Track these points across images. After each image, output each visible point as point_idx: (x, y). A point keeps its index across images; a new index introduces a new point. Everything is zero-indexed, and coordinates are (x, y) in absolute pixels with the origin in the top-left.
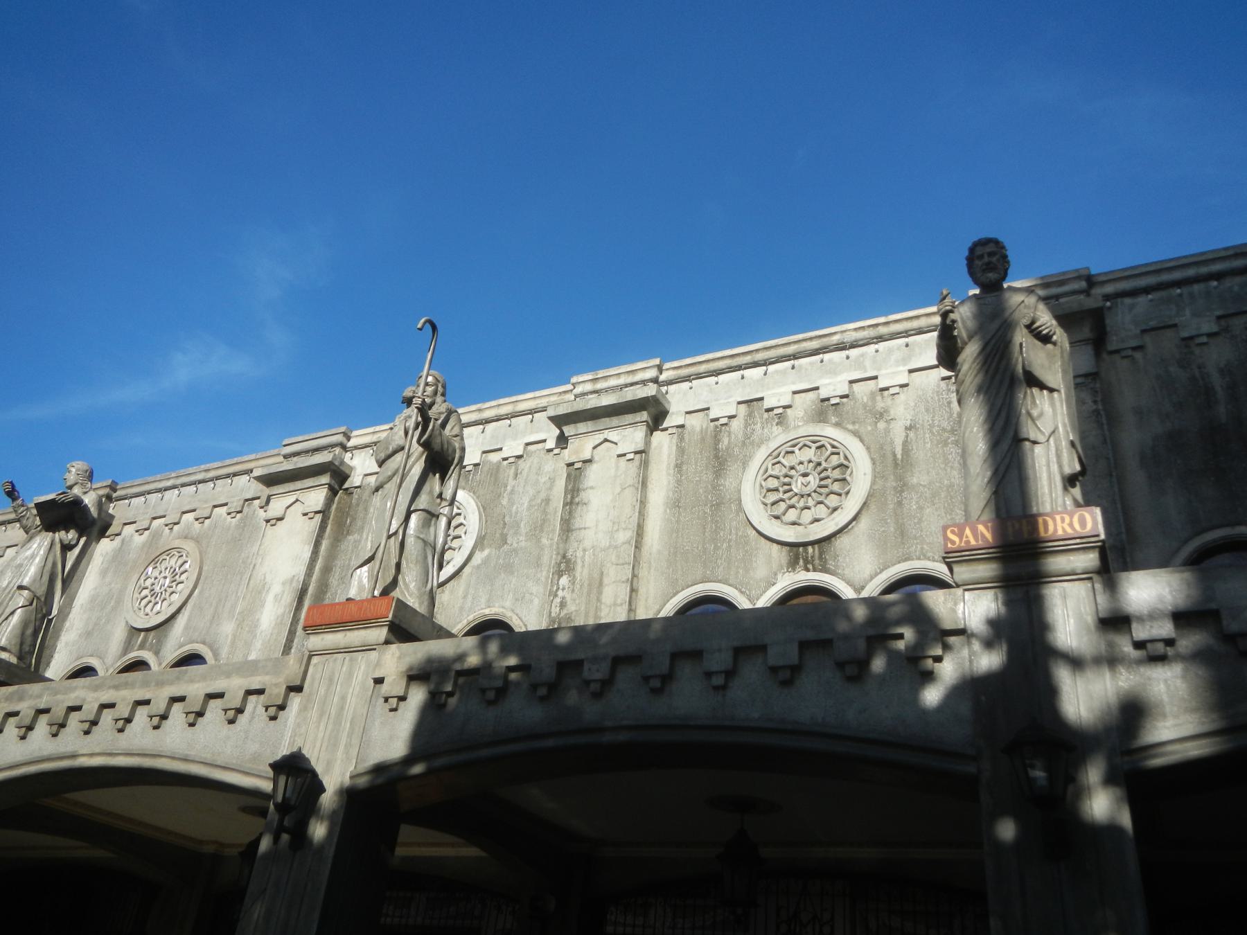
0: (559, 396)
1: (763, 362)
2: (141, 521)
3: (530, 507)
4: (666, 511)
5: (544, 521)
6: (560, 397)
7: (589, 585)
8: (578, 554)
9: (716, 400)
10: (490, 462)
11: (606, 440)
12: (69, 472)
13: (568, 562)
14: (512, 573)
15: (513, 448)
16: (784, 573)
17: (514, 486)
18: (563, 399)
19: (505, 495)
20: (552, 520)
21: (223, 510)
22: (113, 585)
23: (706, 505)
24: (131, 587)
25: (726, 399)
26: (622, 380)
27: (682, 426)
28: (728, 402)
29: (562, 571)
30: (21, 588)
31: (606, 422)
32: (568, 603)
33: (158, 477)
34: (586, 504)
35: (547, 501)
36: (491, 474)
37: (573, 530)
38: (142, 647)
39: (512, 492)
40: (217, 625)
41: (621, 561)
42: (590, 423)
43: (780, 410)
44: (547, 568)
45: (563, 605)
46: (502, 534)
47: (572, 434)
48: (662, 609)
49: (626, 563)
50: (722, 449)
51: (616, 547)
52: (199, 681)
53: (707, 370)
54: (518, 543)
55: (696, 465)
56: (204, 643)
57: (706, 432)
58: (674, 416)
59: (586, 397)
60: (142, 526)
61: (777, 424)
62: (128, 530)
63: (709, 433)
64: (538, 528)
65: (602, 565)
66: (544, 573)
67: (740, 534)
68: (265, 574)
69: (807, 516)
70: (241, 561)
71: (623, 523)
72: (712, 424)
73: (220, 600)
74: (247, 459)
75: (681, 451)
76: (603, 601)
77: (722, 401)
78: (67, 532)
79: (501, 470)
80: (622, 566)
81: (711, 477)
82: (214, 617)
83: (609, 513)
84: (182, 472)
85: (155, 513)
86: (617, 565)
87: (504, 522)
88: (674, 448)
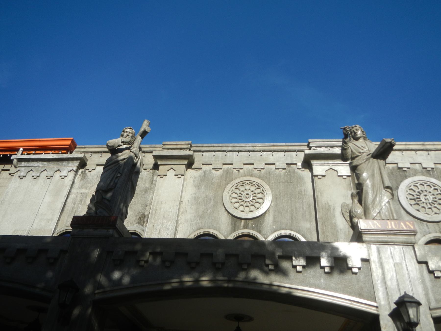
2: (215, 164)
21: (273, 167)
22: (208, 194)
30: (388, 187)
33: (220, 145)
38: (246, 227)
40: (297, 222)
56: (291, 230)
60: (218, 167)
62: (205, 168)
68: (327, 201)
69: (241, 208)
70: (297, 193)
73: (292, 210)
82: (292, 218)
84: (236, 145)
85: (224, 161)
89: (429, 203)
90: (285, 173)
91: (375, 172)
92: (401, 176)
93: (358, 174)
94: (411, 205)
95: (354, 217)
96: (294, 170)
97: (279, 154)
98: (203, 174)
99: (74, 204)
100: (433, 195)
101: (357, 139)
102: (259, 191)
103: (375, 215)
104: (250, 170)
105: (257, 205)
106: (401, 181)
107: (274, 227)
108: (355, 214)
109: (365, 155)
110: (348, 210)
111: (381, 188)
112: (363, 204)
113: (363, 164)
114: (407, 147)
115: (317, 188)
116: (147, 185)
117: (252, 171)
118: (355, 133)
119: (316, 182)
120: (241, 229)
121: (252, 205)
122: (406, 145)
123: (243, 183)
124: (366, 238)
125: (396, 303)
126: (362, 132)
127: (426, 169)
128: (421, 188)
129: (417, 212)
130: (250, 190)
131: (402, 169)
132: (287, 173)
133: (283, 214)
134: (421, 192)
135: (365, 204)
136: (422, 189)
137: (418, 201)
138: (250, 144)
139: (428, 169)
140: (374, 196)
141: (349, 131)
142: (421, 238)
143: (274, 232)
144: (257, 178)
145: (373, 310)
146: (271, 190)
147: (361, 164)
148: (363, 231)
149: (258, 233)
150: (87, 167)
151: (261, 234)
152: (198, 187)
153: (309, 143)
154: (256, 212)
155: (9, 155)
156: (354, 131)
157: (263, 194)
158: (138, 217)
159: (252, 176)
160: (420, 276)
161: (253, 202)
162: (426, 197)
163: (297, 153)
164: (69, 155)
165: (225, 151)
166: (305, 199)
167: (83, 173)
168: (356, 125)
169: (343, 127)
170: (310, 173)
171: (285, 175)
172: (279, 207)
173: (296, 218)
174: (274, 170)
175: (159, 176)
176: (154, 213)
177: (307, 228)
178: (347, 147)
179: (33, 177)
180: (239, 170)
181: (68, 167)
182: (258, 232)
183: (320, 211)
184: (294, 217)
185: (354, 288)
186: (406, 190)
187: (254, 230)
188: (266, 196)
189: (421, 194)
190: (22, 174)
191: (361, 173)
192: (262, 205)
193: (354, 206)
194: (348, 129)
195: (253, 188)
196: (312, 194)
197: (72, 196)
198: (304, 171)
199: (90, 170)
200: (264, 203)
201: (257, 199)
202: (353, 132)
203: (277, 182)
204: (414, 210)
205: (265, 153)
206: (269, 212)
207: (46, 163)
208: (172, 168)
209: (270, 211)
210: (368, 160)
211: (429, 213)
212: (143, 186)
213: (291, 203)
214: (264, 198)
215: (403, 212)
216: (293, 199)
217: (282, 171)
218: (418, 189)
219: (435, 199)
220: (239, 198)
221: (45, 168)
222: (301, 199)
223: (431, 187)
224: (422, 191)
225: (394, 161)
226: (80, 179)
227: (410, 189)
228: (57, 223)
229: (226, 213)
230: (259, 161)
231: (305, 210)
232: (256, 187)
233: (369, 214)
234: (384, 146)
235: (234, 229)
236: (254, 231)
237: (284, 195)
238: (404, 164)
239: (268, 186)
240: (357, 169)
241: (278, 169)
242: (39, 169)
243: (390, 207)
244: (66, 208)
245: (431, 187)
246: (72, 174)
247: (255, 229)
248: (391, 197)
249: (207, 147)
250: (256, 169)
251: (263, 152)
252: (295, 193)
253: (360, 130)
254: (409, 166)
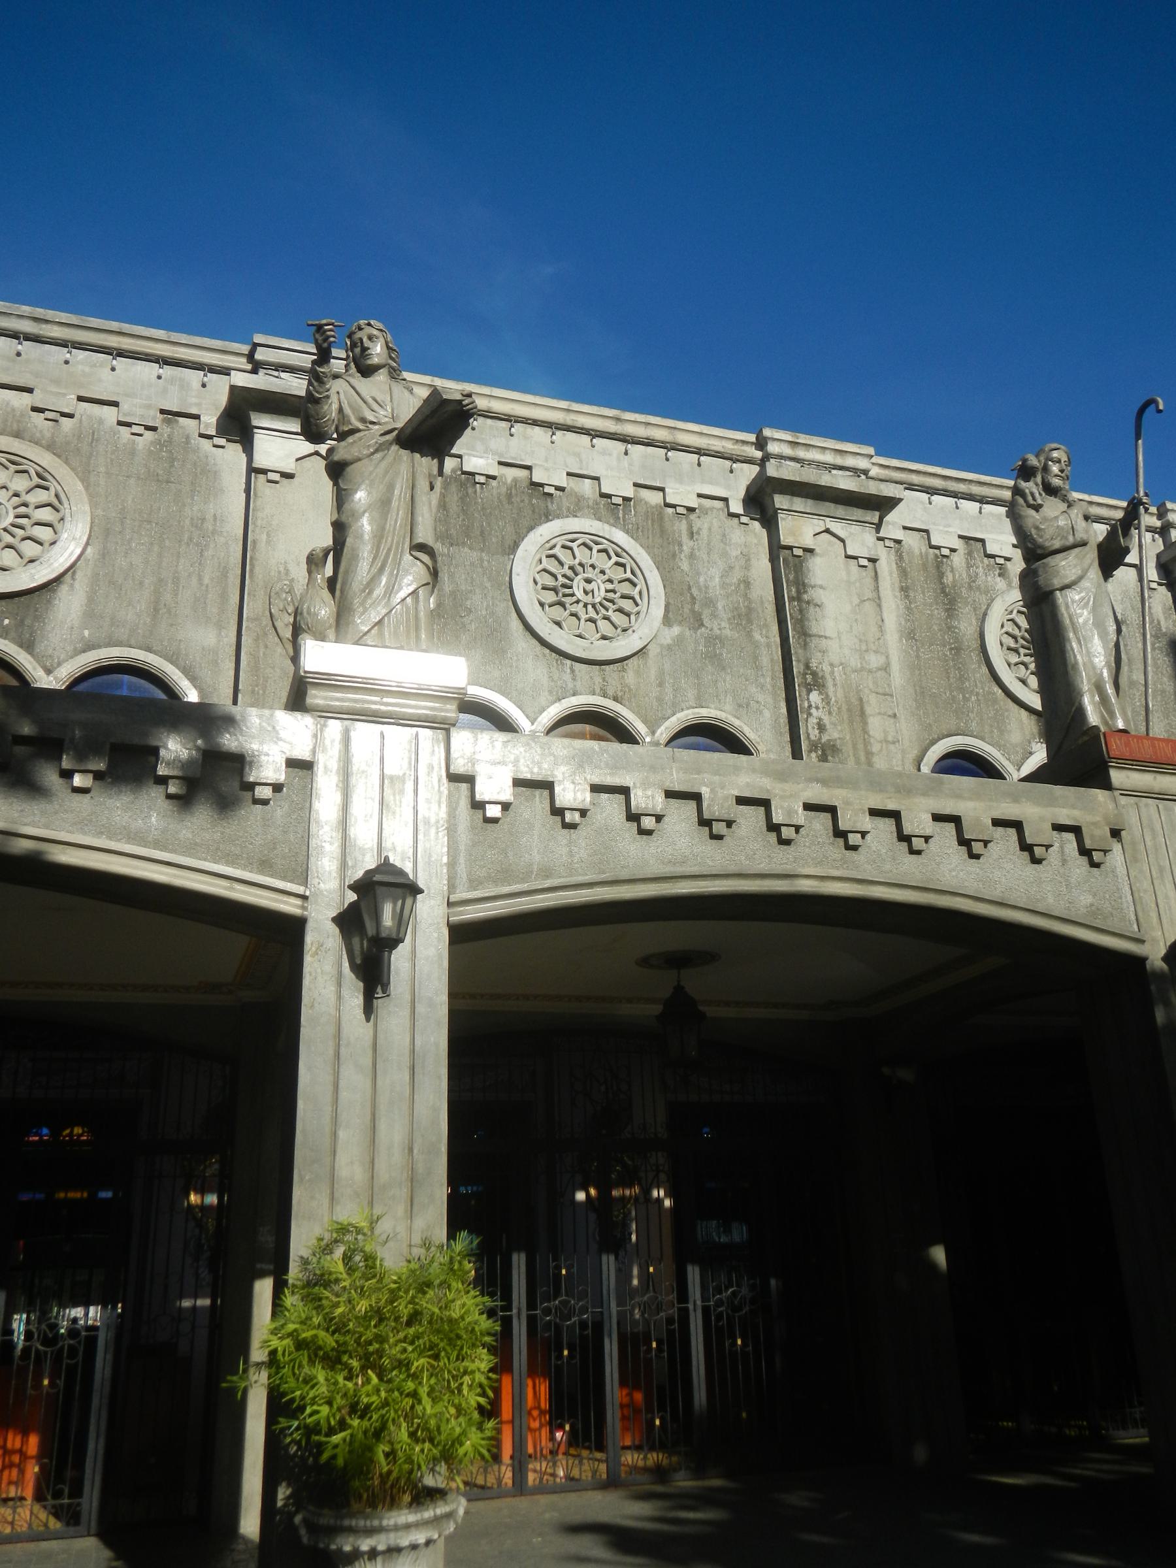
0: (733, 444)
1: (978, 498)
3: (724, 585)
4: (901, 640)
5: (750, 610)
6: (736, 447)
7: (849, 710)
8: (824, 668)
9: (934, 524)
10: (646, 503)
11: (827, 531)
12: (370, 338)
13: (814, 674)
14: (724, 669)
15: (682, 494)
16: (1037, 743)
17: (693, 549)
18: (744, 451)
19: (682, 556)
20: (760, 612)
23: (944, 646)
25: (945, 527)
26: (829, 458)
27: (898, 542)
28: (947, 531)
29: (809, 684)
30: (422, 547)
31: (829, 508)
32: (828, 727)
34: (818, 606)
35: (747, 583)
36: (653, 521)
37: (810, 636)
39: (692, 556)
40: (172, 625)
41: (881, 691)
42: (810, 502)
43: (1001, 561)
44: (770, 673)
45: (821, 727)
46: (692, 611)
47: (785, 508)
48: (924, 756)
49: (888, 695)
50: (948, 585)
51: (870, 671)
52: (971, 799)
53: (921, 483)
54: (720, 629)
55: (923, 593)
56: (149, 650)
57: (927, 558)
58: (890, 526)
59: (783, 461)
61: (1000, 575)
63: (930, 560)
64: (744, 617)
65: (858, 691)
66: (768, 680)
67: (986, 689)
70: (187, 522)
71: (872, 645)
72: (931, 551)
74: (144, 334)
75: (903, 573)
76: (871, 733)
77: (941, 528)
78: (433, 459)
79: (667, 519)
80: (884, 697)
81: (943, 615)
82: (156, 610)
83: (851, 627)
86: (877, 693)
87: (692, 595)
88: (894, 566)
89: (594, 606)
90: (152, 443)
91: (396, 492)
92: (533, 511)
93: (343, 492)
94: (542, 605)
95: (304, 631)
96: (188, 437)
97: (139, 368)
100: (610, 581)
101: (367, 371)
102: (41, 496)
103: (365, 629)
104: (13, 410)
105: (29, 549)
106: (531, 528)
107: (86, 633)
108: (309, 620)
109: (377, 430)
110: (294, 604)
111: (403, 548)
112: (338, 593)
113: (363, 461)
114: (570, 419)
115: (259, 514)
117: (22, 415)
118: (364, 349)
119: (259, 494)
122: (568, 410)
124: (315, 697)
125: (354, 887)
126: (388, 348)
127: (609, 500)
128: (581, 555)
129: (556, 628)
130: (8, 490)
131: (541, 489)
132: (162, 446)
133: (126, 590)
134: (580, 569)
135: (342, 591)
136: (584, 561)
137: (565, 595)
138: (26, 309)
139: (615, 500)
140: (374, 570)
141: (332, 339)
142: (548, 707)
143: (84, 651)
144: (41, 446)
145: (289, 906)
146: (90, 502)
147: (359, 460)
148: (311, 675)
149: (20, 650)
151: (35, 653)
153: (255, 346)
154: (23, 576)
156: (361, 340)
157: (58, 511)
159: (23, 439)
160: (445, 816)
161: (13, 536)
162: (589, 587)
163: (205, 375)
166: (212, 546)
168: (372, 322)
169: (317, 322)
170: (243, 458)
171: (150, 452)
172: (114, 565)
173: (169, 612)
174: (111, 428)
177: (203, 649)
178: (323, 392)
182: (21, 646)
183: (254, 596)
184: (165, 605)
185: (251, 844)
186: (537, 557)
187: (5, 639)
188: (68, 518)
189: (576, 574)
191: (351, 489)
192: (48, 551)
193: (309, 595)
194: (332, 333)
195: (20, 484)
196: (241, 531)
198: (223, 447)
200: (58, 543)
201: (32, 526)
202: (359, 344)
203: (117, 475)
204: (546, 620)
205: (81, 355)
206: (73, 579)
209: (79, 575)
210: (383, 450)
211: (587, 636)
213: (160, 555)
214: (58, 526)
215: (515, 623)
216: (167, 543)
217: (141, 435)
218: (575, 558)
219: (611, 595)
222: (197, 545)
223: (610, 558)
224: (581, 564)
225: (521, 460)
227: (548, 556)
230: (57, 382)
231: (207, 586)
232: (31, 480)
233: (348, 624)
234: (434, 412)
236: (6, 642)
237: (137, 523)
238: (551, 474)
239: (79, 483)
240: (345, 473)
241: (129, 425)
243: (416, 609)
245: (610, 558)
247: (13, 634)
248: (426, 578)
250: (40, 410)
251: (73, 350)
252: (179, 522)
253: (382, 340)
254: (562, 481)
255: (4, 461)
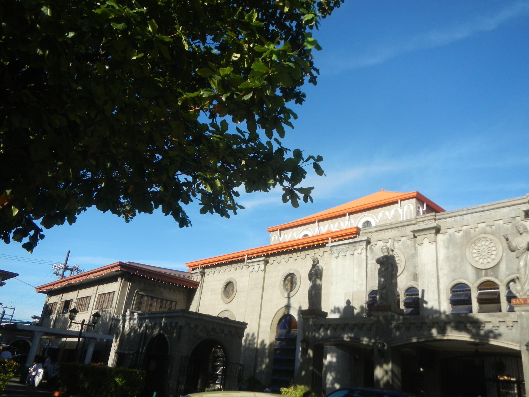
21: (501, 222)
24: (468, 254)
38: (486, 275)
62: (450, 231)
74: (503, 202)
98: (449, 237)
99: (372, 271)
102: (492, 245)
116: (413, 251)
120: (483, 277)
121: (489, 257)
123: (479, 240)
140: (525, 280)
150: (372, 243)
152: (447, 248)
155: (324, 243)
158: (413, 276)
164: (358, 239)
165: (461, 215)
167: (371, 248)
175: (418, 244)
176: (421, 272)
179: (343, 256)
180: (474, 229)
181: (360, 246)
190: (336, 255)
197: (369, 266)
199: (374, 246)
207: (346, 246)
208: (426, 237)
212: (410, 252)
220: (479, 252)
221: (348, 249)
226: (370, 253)
228: (366, 286)
229: (470, 266)
235: (478, 277)
242: (345, 250)
244: (368, 275)
246: (364, 251)
249: (447, 214)
255: (483, 239)
